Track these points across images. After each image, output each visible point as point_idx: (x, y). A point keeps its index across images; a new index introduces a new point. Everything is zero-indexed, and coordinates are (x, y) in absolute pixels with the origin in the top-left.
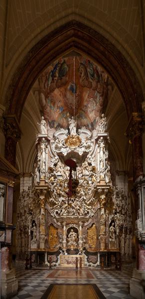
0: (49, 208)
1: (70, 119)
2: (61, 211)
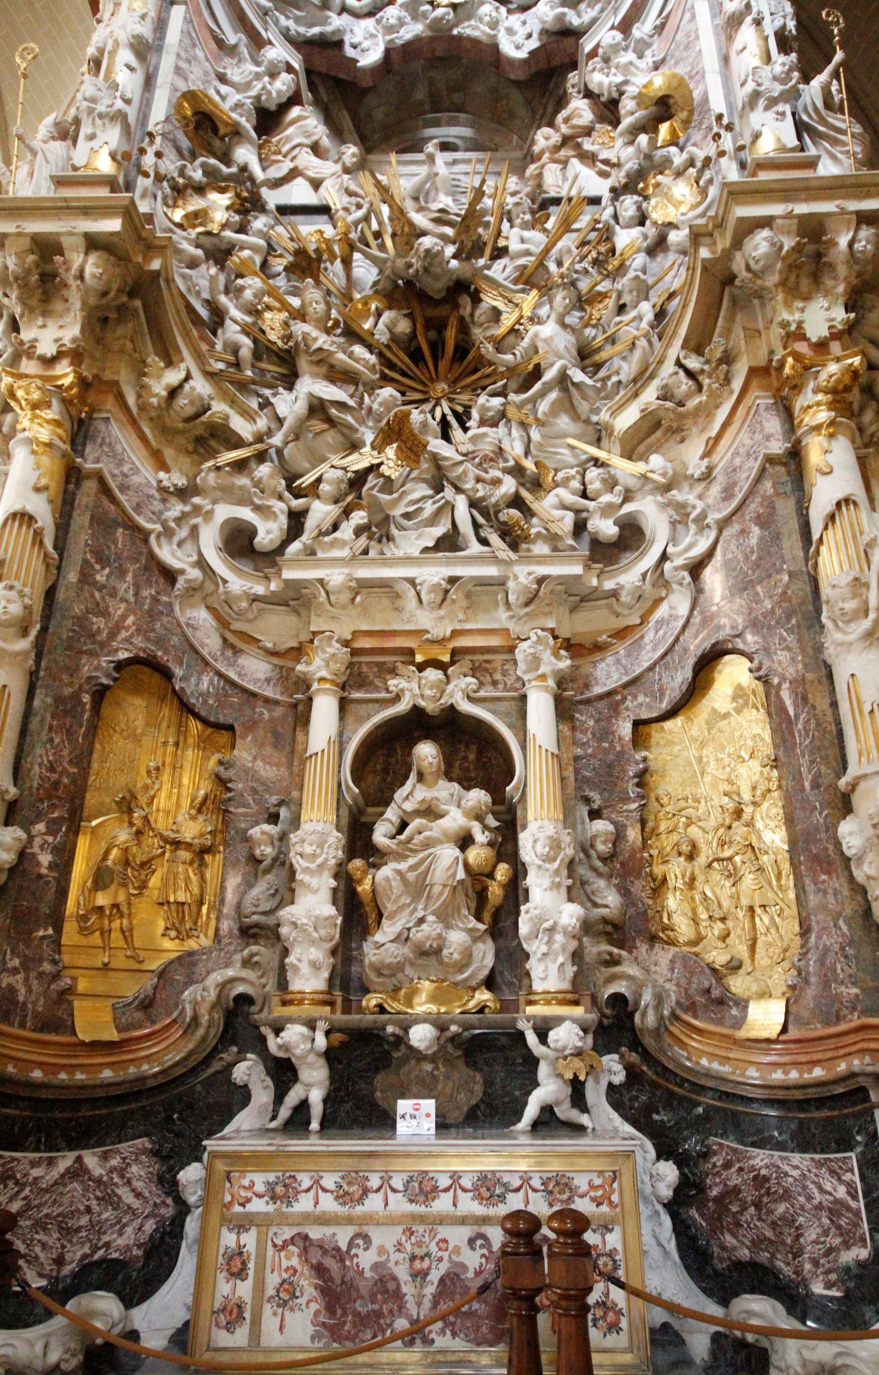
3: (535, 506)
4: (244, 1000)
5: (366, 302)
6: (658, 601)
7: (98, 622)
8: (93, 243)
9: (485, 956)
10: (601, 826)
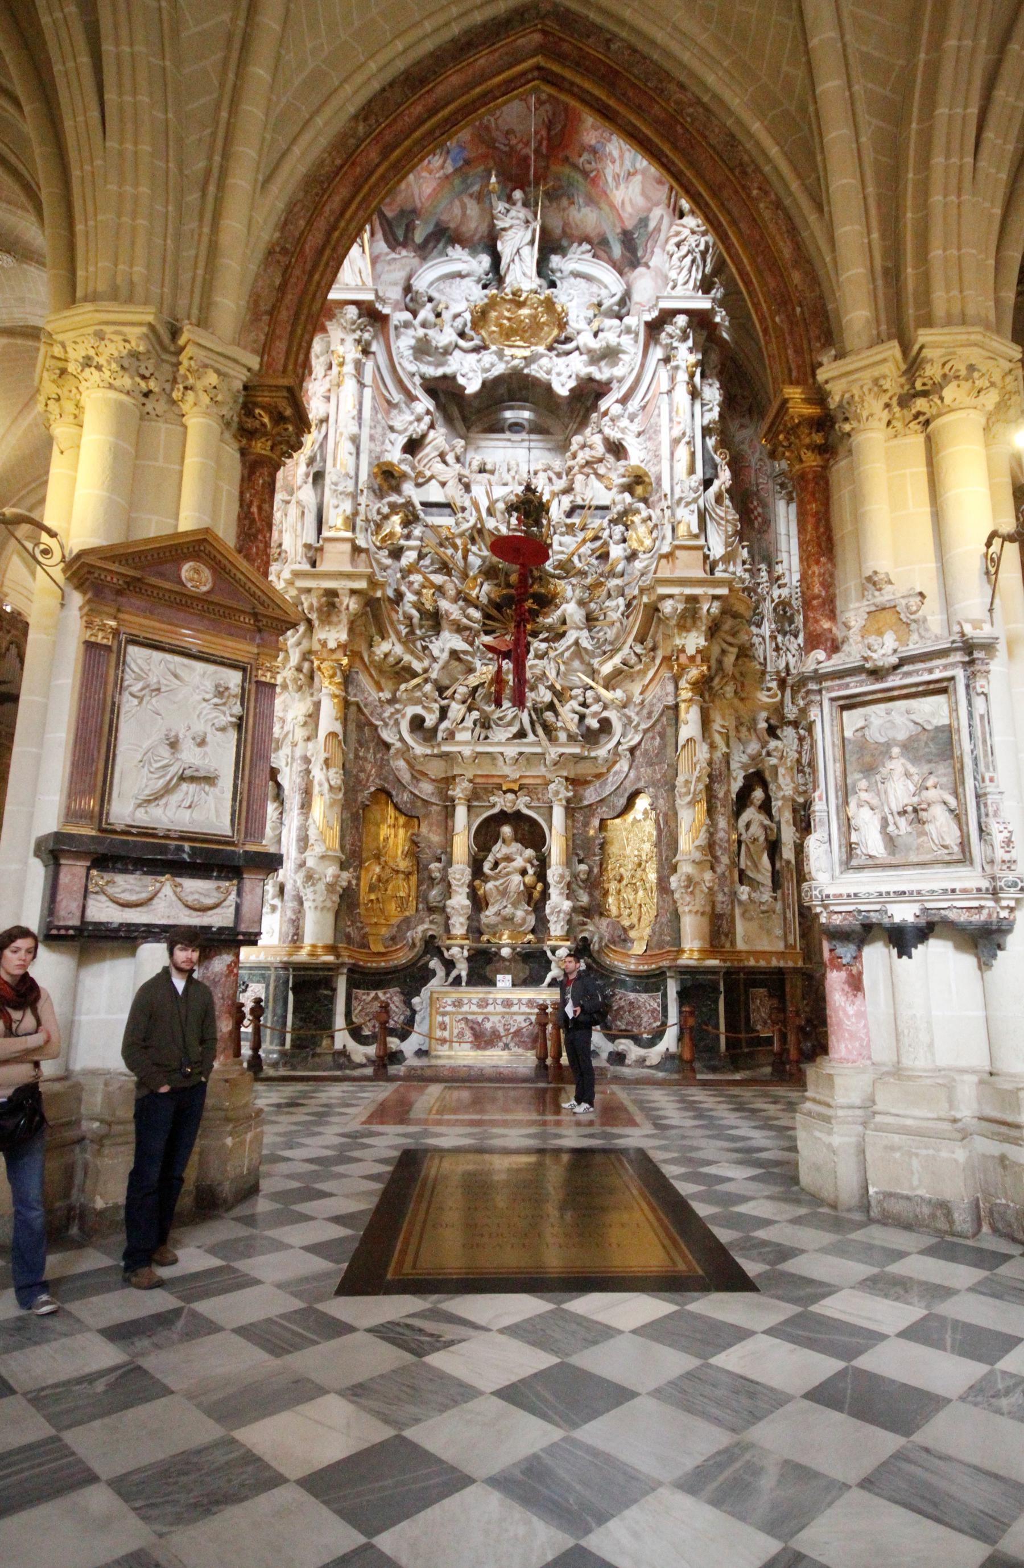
0: (370, 692)
1: (501, 206)
2: (444, 712)
3: (560, 709)
4: (432, 937)
5: (475, 578)
6: (615, 762)
7: (362, 775)
8: (353, 592)
9: (531, 920)
10: (583, 867)
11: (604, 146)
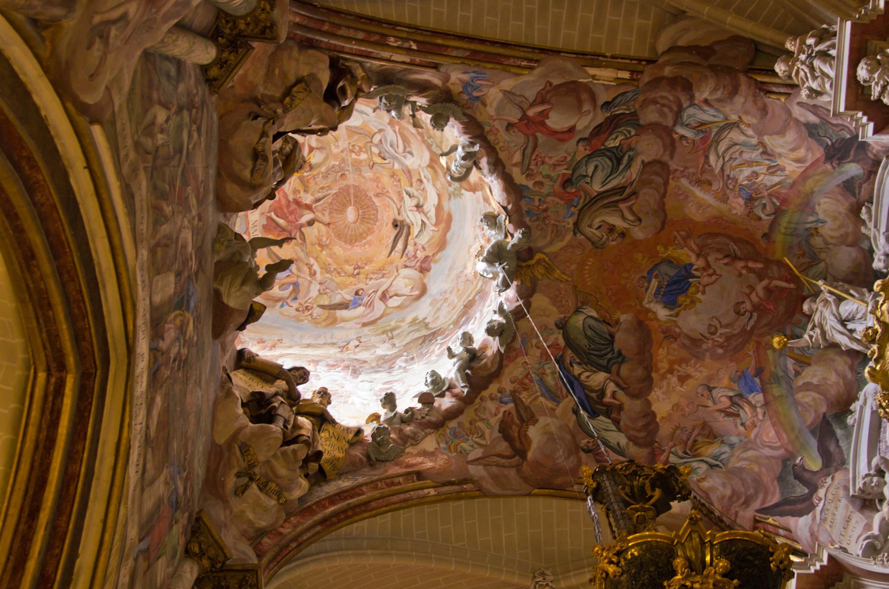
11: (742, 188)
